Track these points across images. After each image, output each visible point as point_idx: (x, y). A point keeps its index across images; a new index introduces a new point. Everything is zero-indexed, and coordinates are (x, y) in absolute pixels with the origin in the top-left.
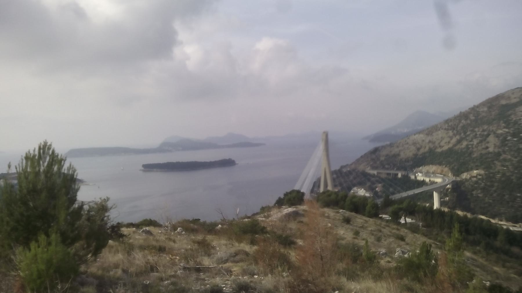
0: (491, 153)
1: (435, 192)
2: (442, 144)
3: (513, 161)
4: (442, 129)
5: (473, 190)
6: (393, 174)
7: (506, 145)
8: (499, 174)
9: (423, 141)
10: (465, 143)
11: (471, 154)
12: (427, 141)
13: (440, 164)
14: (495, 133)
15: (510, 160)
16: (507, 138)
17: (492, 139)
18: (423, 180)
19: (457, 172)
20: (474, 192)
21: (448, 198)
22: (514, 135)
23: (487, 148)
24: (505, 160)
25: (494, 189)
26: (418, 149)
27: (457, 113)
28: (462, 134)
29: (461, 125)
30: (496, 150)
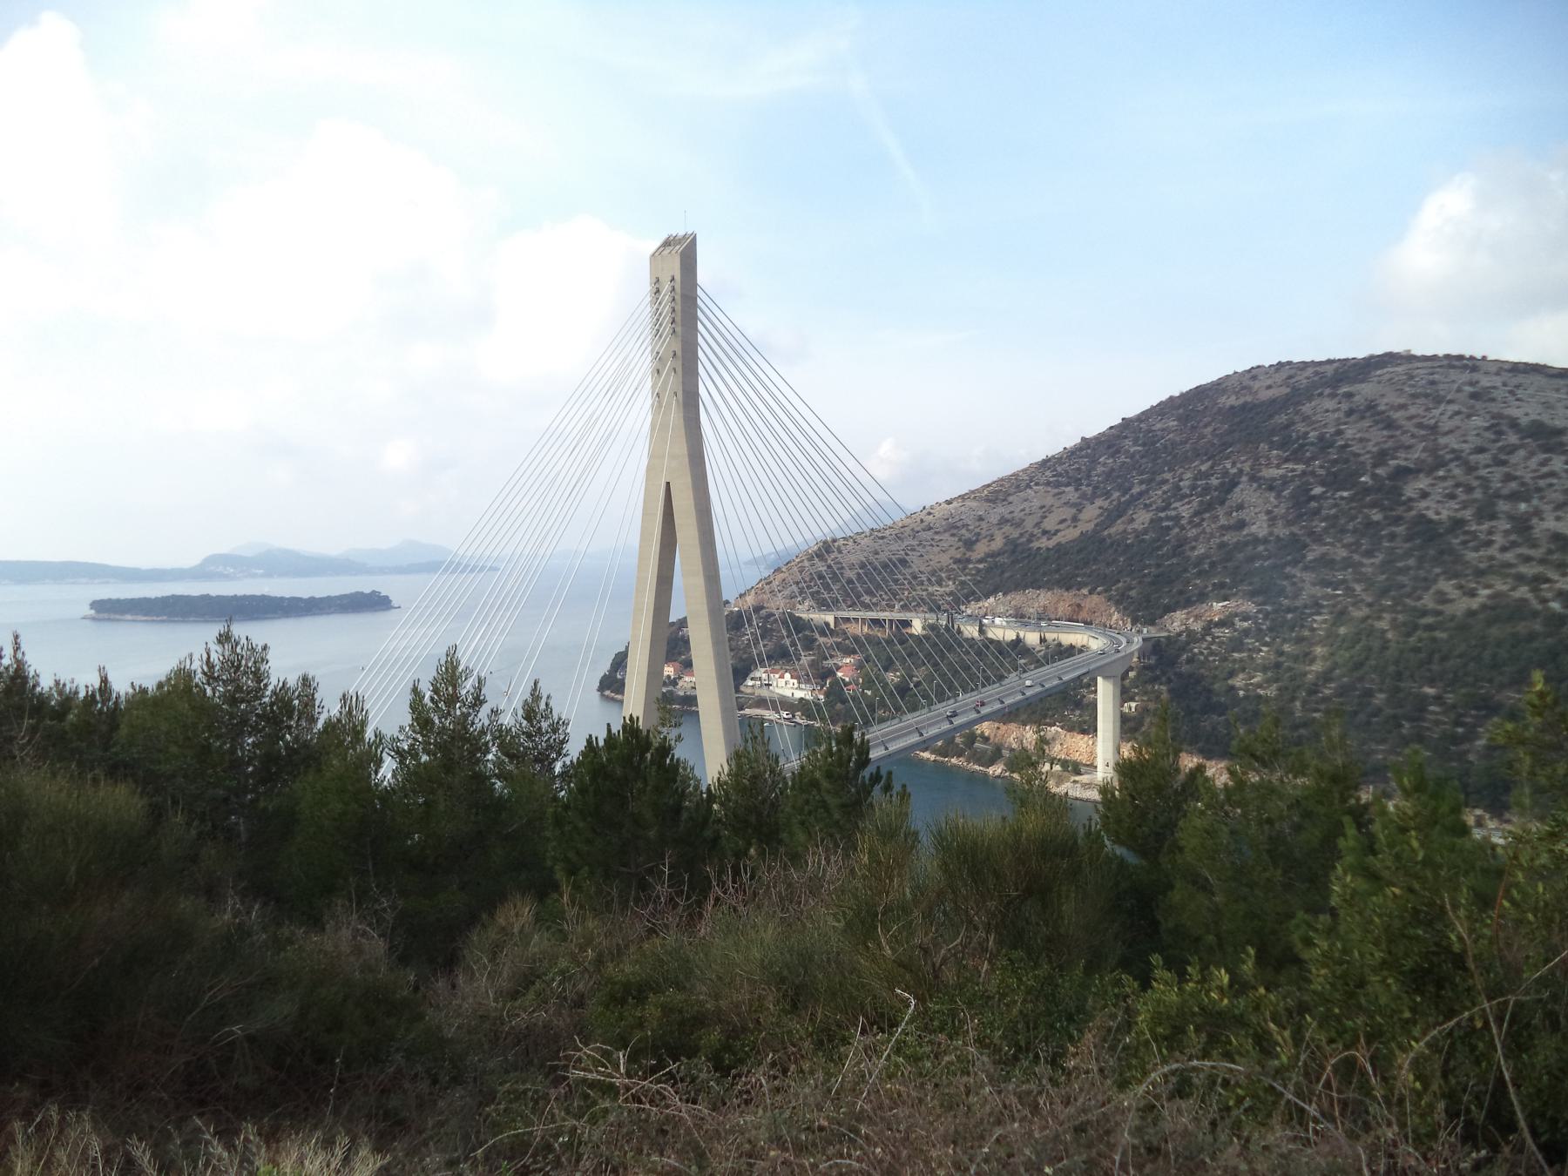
0: (1265, 541)
1: (1105, 678)
2: (1049, 524)
3: (1362, 565)
4: (1037, 484)
5: (1232, 674)
6: (891, 621)
7: (1316, 512)
8: (1319, 614)
9: (981, 519)
10: (1142, 518)
11: (1182, 543)
12: (994, 519)
13: (1067, 584)
14: (1253, 478)
15: (1347, 563)
16: (1311, 489)
17: (1245, 493)
18: (1014, 638)
19: (1145, 610)
20: (1238, 681)
21: (1133, 705)
22: (1334, 481)
23: (1241, 525)
24: (1326, 562)
25: (1317, 667)
26: (970, 544)
27: (1072, 441)
28: (1116, 494)
29: (1100, 469)
30: (1282, 531)
